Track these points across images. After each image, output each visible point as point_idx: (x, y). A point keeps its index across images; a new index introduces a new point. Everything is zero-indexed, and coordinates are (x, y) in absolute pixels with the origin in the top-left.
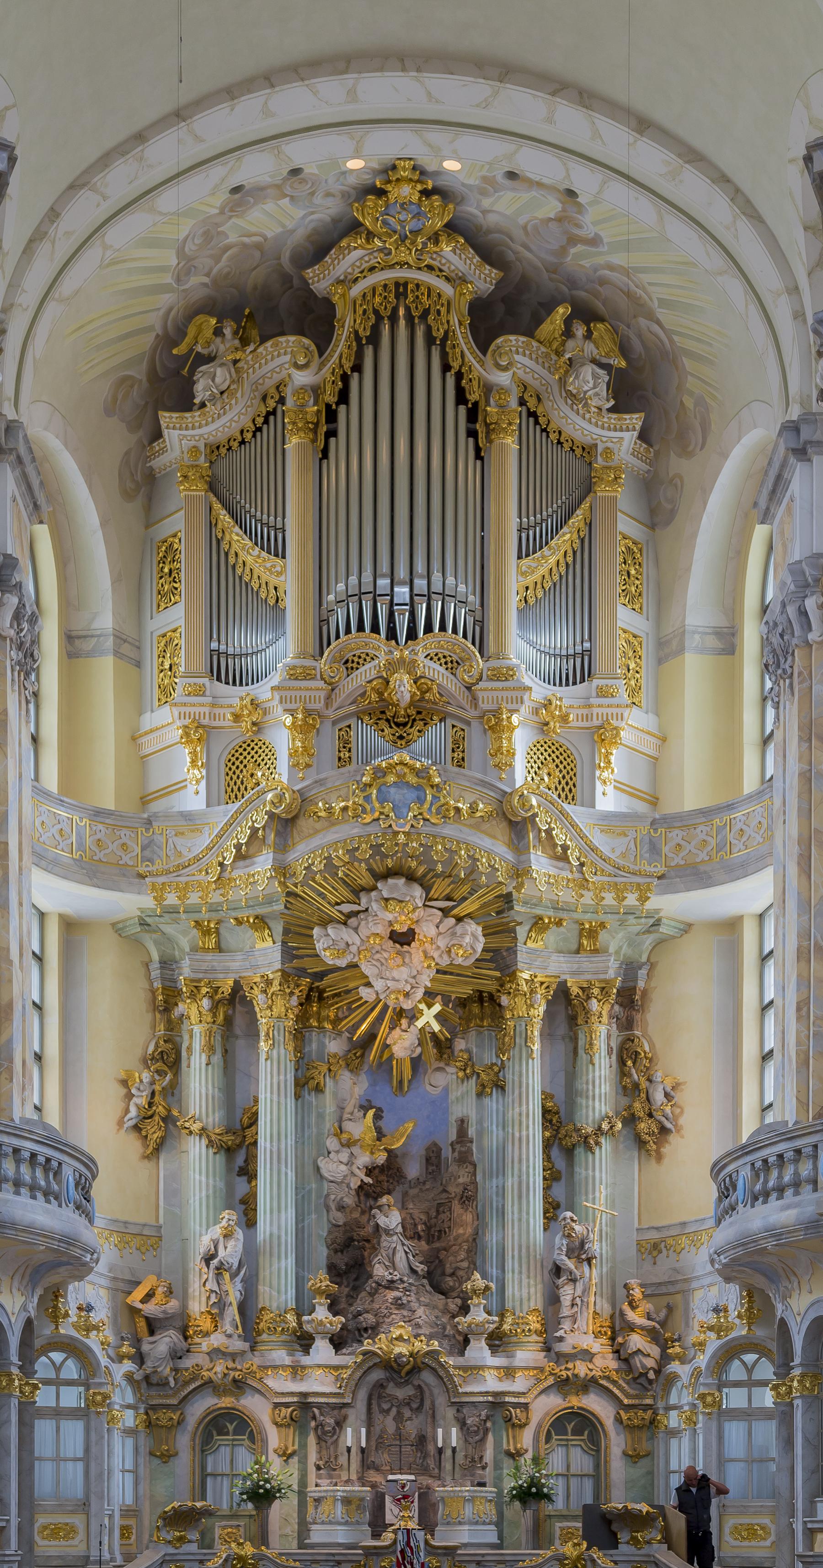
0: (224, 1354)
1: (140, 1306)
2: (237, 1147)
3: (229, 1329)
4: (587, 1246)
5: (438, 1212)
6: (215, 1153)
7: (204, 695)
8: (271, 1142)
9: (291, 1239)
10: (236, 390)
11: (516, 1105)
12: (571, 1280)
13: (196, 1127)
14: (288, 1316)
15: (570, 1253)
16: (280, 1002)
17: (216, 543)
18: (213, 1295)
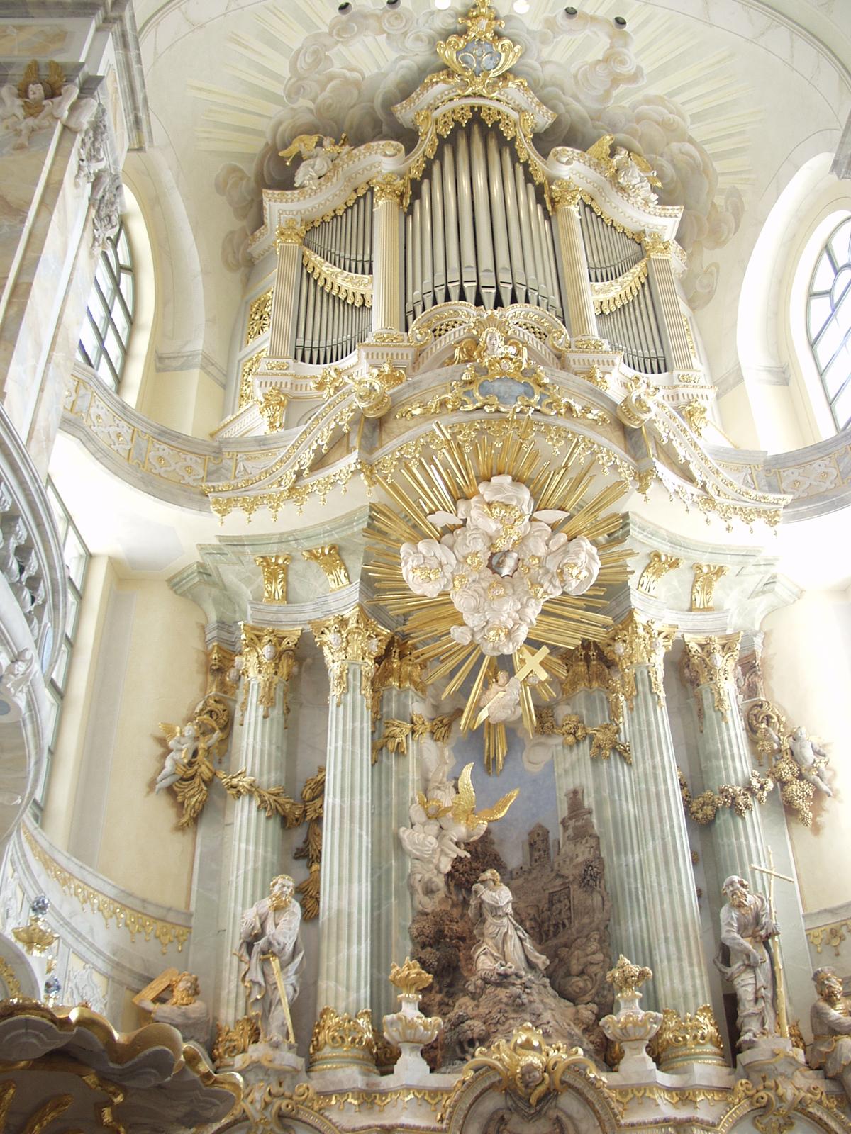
0: (267, 1071)
1: (149, 1006)
2: (297, 823)
3: (276, 1036)
4: (764, 920)
5: (551, 903)
6: (268, 818)
7: (287, 369)
8: (342, 797)
9: (365, 920)
10: (332, 177)
11: (648, 756)
12: (748, 966)
13: (244, 782)
14: (361, 1021)
15: (742, 929)
16: (357, 643)
17: (307, 275)
18: (256, 988)
